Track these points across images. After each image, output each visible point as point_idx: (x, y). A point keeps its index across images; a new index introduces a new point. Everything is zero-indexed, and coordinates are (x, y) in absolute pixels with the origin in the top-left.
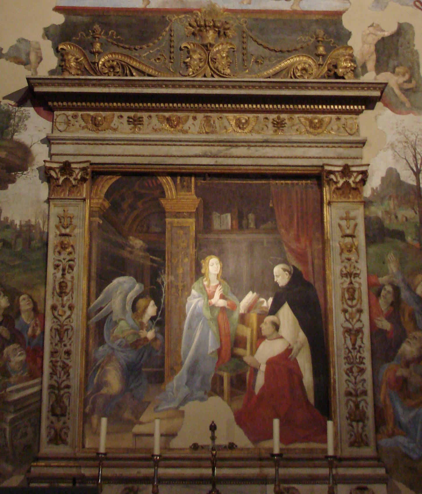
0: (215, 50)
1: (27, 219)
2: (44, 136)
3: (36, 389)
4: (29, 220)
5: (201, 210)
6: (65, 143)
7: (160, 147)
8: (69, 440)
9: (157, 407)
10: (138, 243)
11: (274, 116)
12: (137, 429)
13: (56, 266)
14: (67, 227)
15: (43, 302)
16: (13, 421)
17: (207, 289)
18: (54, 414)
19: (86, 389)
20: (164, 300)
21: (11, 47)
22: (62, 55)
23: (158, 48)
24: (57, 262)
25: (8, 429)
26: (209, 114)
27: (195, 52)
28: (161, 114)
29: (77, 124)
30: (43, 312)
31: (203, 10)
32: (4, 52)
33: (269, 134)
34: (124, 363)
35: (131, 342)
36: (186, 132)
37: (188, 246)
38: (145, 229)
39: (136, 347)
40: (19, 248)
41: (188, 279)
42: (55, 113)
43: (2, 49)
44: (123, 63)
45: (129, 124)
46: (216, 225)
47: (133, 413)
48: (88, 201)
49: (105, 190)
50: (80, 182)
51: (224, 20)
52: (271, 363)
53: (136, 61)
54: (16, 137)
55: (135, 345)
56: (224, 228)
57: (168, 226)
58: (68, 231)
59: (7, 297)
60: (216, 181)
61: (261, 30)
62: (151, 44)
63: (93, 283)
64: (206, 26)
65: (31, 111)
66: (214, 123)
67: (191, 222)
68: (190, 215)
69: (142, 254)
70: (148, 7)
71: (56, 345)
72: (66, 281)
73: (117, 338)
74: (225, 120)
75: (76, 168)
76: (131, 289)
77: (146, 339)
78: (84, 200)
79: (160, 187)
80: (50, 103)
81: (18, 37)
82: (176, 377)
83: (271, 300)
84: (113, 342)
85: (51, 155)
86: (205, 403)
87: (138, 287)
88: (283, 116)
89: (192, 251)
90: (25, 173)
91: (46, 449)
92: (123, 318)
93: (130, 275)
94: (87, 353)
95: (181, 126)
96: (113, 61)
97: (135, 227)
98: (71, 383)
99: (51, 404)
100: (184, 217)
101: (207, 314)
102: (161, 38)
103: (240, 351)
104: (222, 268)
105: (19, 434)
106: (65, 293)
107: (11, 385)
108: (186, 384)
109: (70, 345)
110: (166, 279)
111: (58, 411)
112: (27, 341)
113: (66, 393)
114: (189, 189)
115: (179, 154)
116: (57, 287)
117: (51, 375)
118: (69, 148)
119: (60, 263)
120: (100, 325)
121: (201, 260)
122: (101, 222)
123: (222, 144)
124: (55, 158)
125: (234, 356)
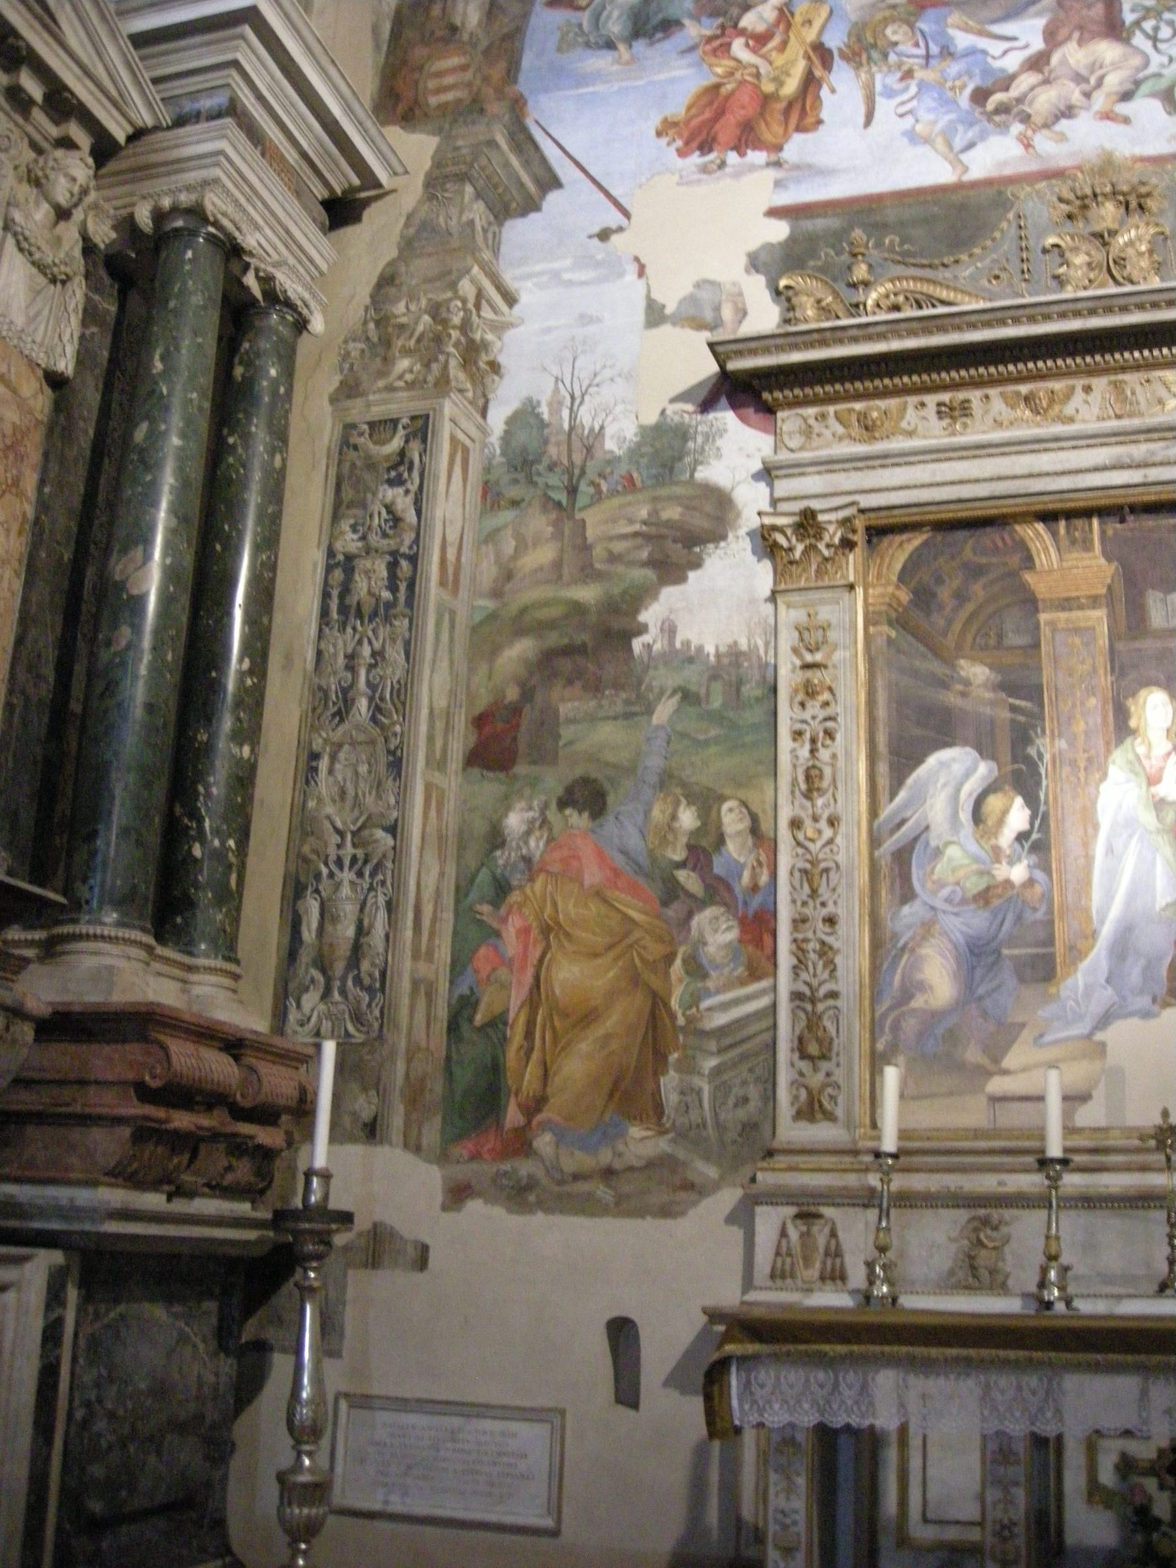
0: (1122, 240)
1: (730, 641)
2: (758, 466)
3: (765, 1001)
4: (736, 643)
5: (1119, 589)
6: (802, 474)
7: (1014, 458)
8: (840, 1112)
9: (1041, 1036)
10: (977, 672)
12: (997, 1085)
13: (797, 735)
14: (818, 649)
15: (771, 813)
16: (717, 1071)
17: (1146, 763)
18: (804, 1056)
19: (875, 999)
20: (1047, 795)
21: (685, 299)
22: (789, 300)
23: (995, 256)
24: (798, 726)
26: (1120, 377)
27: (1075, 250)
28: (1010, 388)
29: (827, 433)
30: (772, 835)
31: (1087, 167)
32: (668, 311)
34: (961, 940)
35: (975, 891)
36: (1071, 420)
37: (1095, 669)
38: (992, 642)
39: (987, 902)
40: (716, 703)
41: (1101, 743)
42: (780, 415)
43: (664, 306)
44: (918, 296)
45: (940, 418)
47: (986, 1050)
48: (860, 591)
49: (898, 566)
50: (840, 552)
51: (1135, 180)
53: (948, 287)
54: (701, 474)
55: (984, 897)
57: (1045, 631)
58: (818, 657)
59: (694, 808)
60: (1150, 522)
62: (977, 251)
63: (883, 768)
64: (1095, 195)
65: (726, 417)
66: (1133, 393)
67: (1098, 617)
68: (1094, 602)
69: (988, 695)
70: (966, 178)
71: (804, 904)
72: (818, 764)
73: (941, 885)
75: (830, 522)
76: (967, 775)
77: (1008, 883)
79: (1022, 547)
80: (766, 396)
81: (696, 278)
82: (1084, 965)
84: (934, 893)
85: (774, 502)
86: (1152, 1023)
87: (984, 770)
89: (1104, 680)
90: (722, 544)
91: (790, 1131)
92: (955, 839)
93: (965, 743)
94: (875, 923)
95: (1057, 408)
96: (896, 294)
97: (969, 638)
98: (841, 987)
99: (797, 1032)
100: (1081, 607)
101: (1148, 818)
102: (997, 235)
105: (731, 1102)
106: (818, 789)
107: (708, 994)
108: (1108, 981)
109: (835, 903)
110: (1046, 747)
111: (813, 1049)
112: (740, 897)
113: (830, 1008)
114: (1087, 546)
115: (1059, 467)
116: (801, 778)
117: (795, 970)
118: (812, 483)
119: (804, 726)
120: (903, 857)
121: (1126, 698)
122: (893, 634)
123: (1155, 435)
124: (783, 507)
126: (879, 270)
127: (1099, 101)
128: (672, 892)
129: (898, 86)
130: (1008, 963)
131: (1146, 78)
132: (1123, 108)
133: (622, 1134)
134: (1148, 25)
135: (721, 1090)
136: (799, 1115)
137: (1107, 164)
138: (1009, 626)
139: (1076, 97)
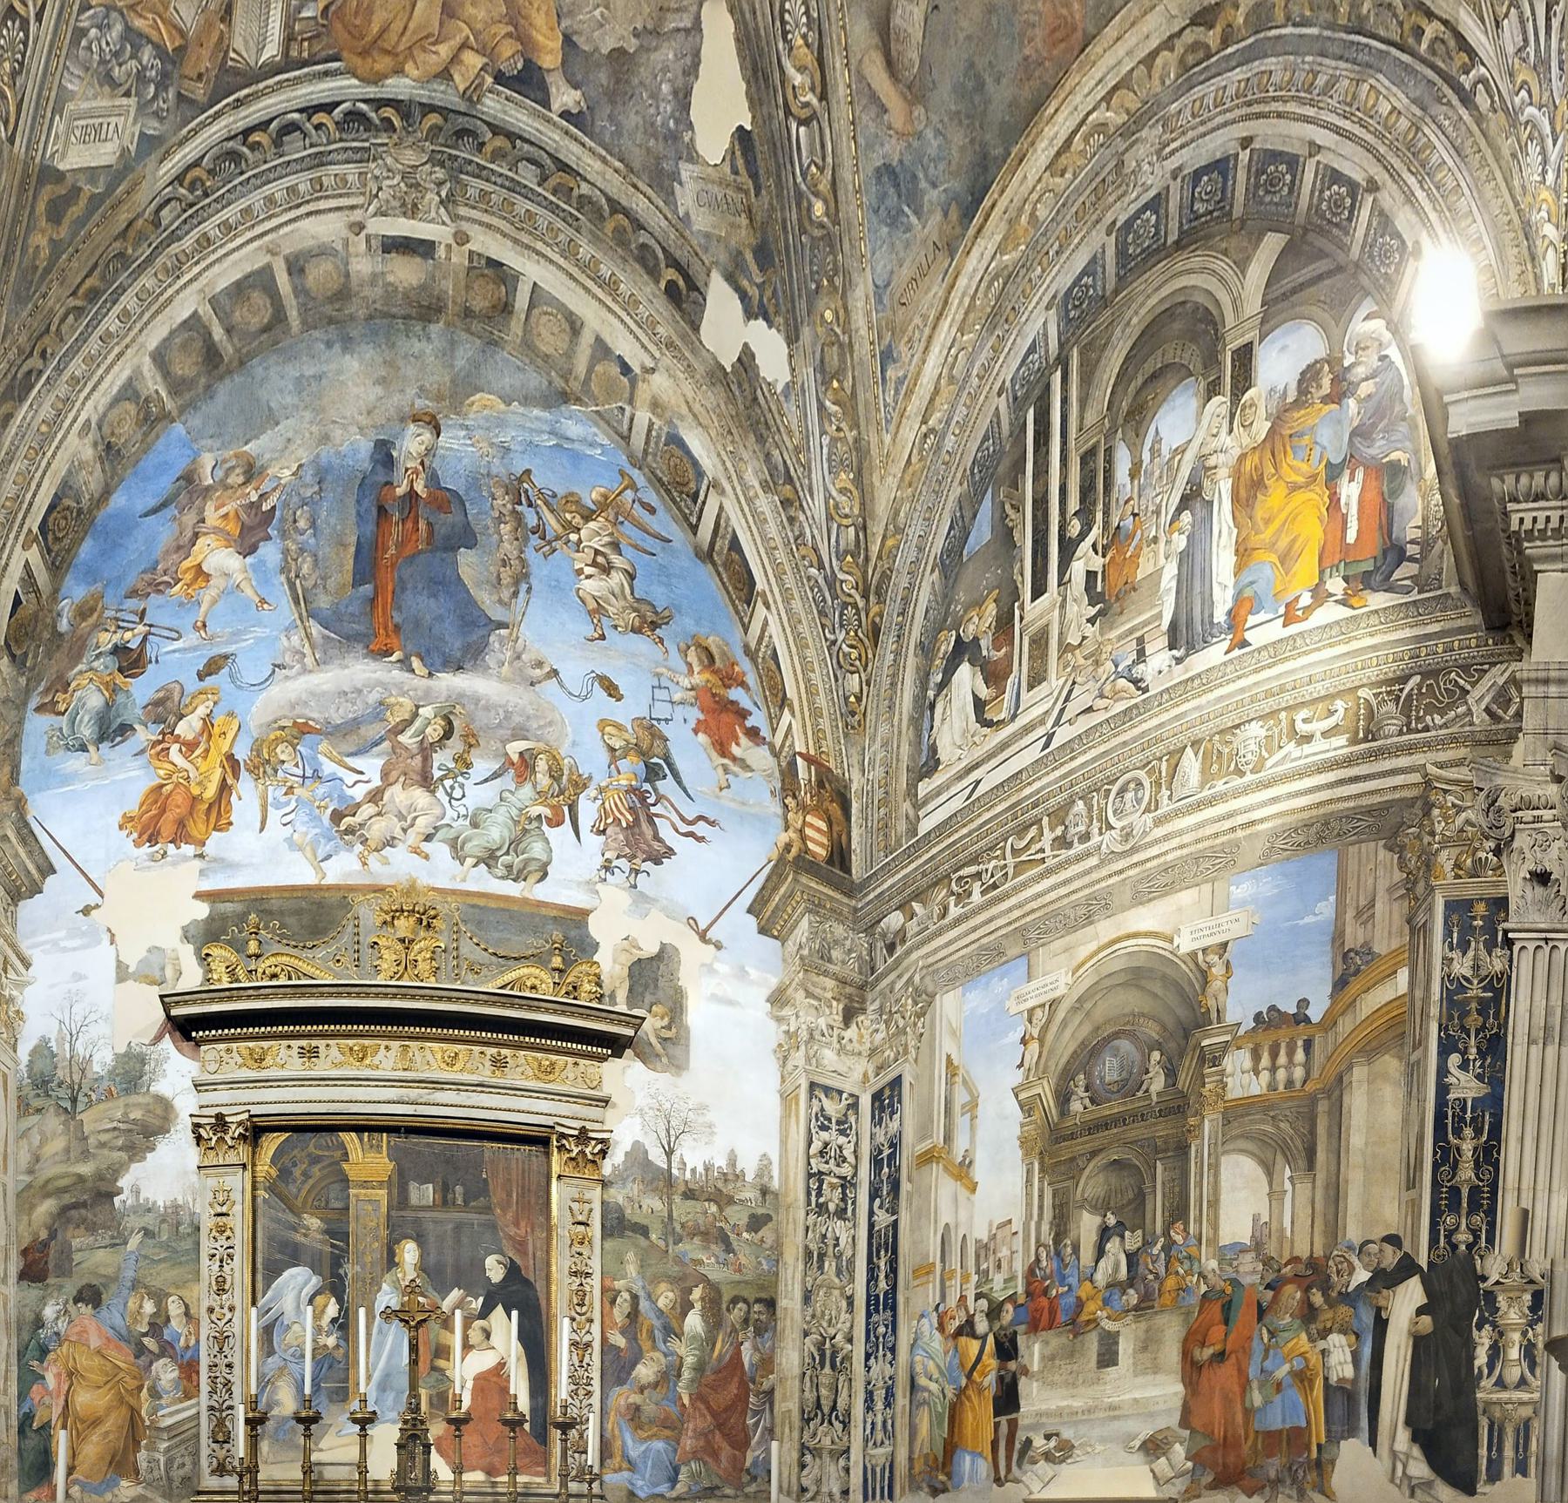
3: (193, 1411)
5: (395, 1178)
10: (313, 1222)
11: (494, 1051)
16: (168, 1449)
18: (216, 1442)
25: (162, 1460)
33: (486, 1074)
46: (414, 1199)
52: (481, 1380)
56: (424, 1203)
57: (353, 1200)
58: (224, 1209)
60: (415, 1139)
61: (480, 922)
74: (428, 1052)
76: (306, 1284)
78: (244, 1166)
79: (342, 1146)
83: (481, 1299)
87: (315, 1281)
88: (504, 1052)
89: (384, 1233)
103: (441, 1363)
104: (421, 1256)
110: (350, 1270)
111: (220, 1437)
118: (222, 1096)
125: (434, 1368)
126: (265, 946)
127: (412, 837)
128: (140, 1350)
129: (284, 799)
130: (324, 1392)
131: (443, 826)
132: (426, 847)
133: (117, 1485)
134: (448, 783)
135: (170, 1462)
136: (213, 1472)
137: (411, 889)
138: (332, 1195)
139: (398, 832)
